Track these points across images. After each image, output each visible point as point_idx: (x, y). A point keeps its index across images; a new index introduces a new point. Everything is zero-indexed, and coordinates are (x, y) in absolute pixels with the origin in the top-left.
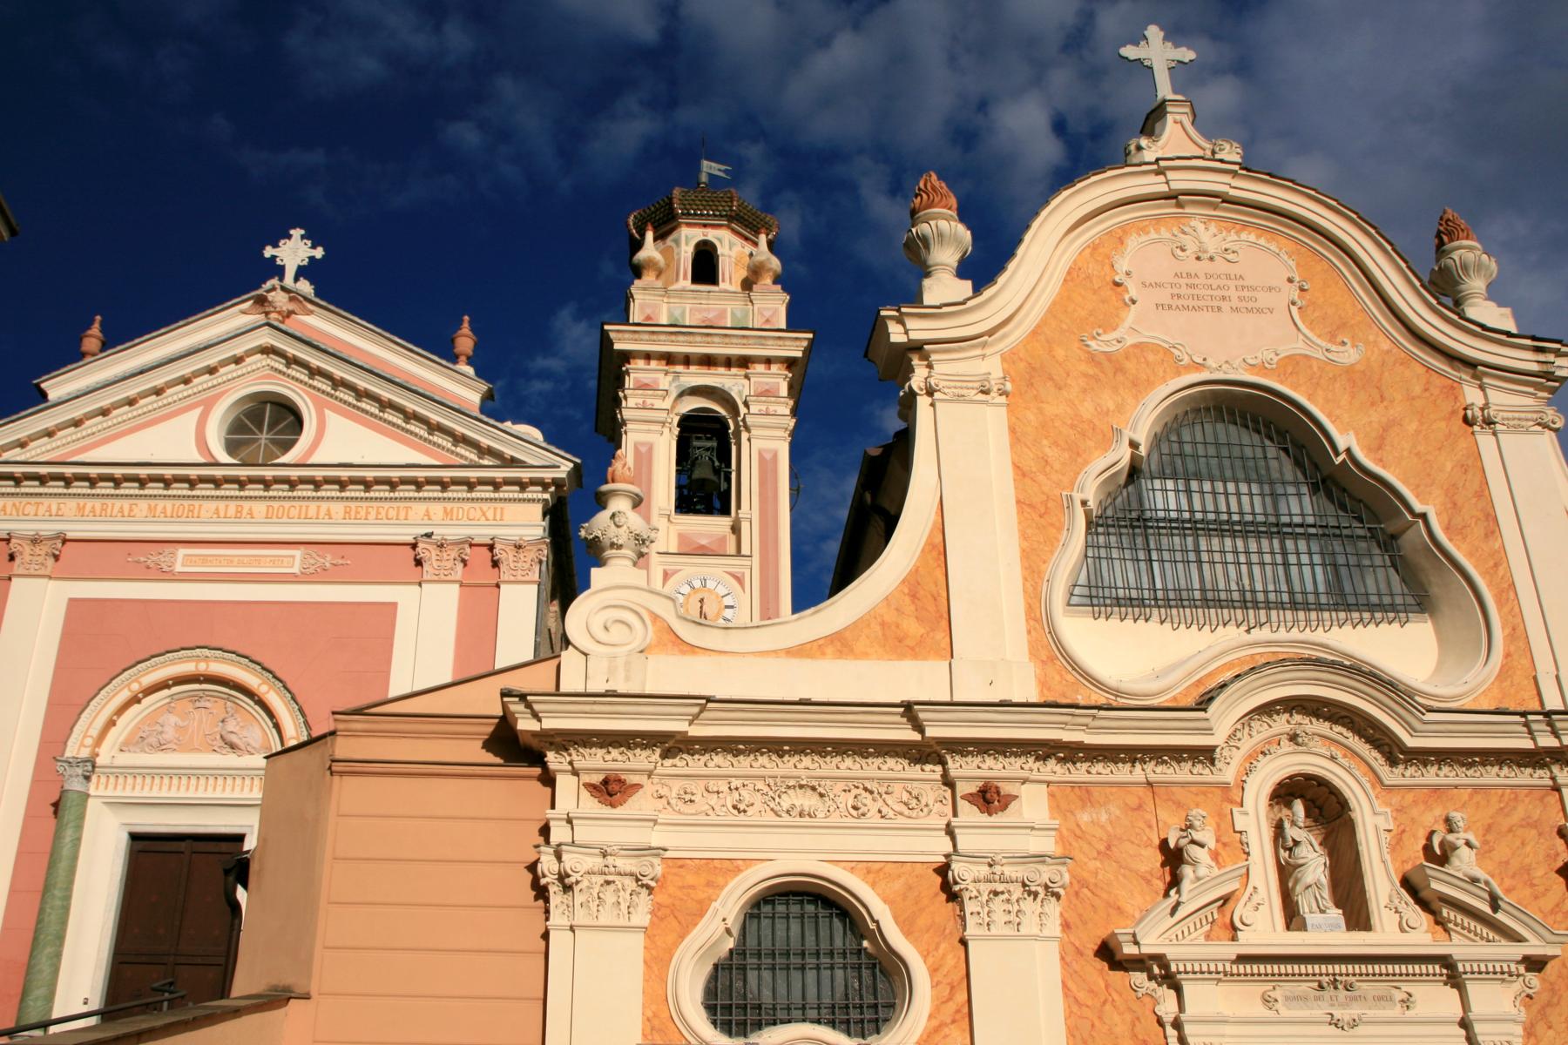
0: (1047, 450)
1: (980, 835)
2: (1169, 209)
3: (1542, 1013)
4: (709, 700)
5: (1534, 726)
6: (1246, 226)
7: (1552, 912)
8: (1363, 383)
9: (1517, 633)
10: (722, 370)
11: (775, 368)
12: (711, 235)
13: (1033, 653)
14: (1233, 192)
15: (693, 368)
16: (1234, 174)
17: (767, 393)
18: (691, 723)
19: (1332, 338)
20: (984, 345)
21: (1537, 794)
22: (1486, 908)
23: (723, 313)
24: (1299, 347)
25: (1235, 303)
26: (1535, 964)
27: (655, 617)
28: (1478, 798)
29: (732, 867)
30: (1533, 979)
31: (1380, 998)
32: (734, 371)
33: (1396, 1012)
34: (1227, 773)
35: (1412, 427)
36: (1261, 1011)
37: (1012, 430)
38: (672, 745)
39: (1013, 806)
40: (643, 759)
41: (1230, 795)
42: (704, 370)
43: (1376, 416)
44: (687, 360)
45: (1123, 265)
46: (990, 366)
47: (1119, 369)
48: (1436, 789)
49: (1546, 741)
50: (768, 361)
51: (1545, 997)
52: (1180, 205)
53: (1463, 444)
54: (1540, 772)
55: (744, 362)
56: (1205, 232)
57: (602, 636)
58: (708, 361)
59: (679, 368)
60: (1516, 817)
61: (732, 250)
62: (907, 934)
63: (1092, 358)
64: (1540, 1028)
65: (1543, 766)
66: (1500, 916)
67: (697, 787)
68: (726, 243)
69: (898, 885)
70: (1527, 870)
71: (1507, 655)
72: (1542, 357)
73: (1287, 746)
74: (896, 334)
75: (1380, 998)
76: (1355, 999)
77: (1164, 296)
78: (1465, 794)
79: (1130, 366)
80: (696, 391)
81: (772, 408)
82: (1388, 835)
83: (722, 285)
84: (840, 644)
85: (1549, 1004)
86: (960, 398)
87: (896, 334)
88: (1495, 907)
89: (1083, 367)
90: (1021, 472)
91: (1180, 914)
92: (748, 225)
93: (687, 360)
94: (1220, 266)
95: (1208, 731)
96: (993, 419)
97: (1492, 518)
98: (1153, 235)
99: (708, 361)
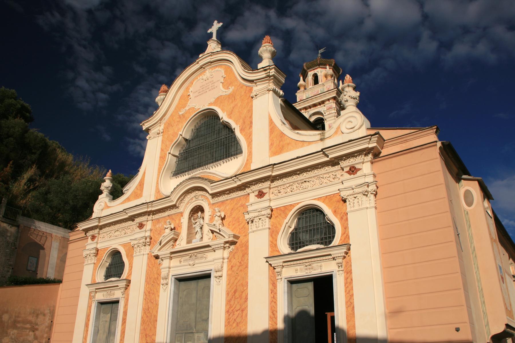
0: (167, 143)
1: (140, 234)
2: (202, 70)
3: (234, 255)
4: (100, 218)
5: (235, 180)
6: (216, 67)
7: (242, 228)
8: (231, 97)
9: (250, 153)
10: (319, 106)
11: (331, 101)
12: (315, 71)
13: (156, 191)
14: (212, 60)
15: (312, 109)
16: (211, 55)
17: (330, 108)
18: (99, 222)
19: (228, 88)
20: (160, 123)
21: (245, 197)
22: (218, 231)
23: (318, 91)
24: (221, 94)
25: (210, 88)
26: (233, 243)
27: (106, 202)
28: (232, 202)
29: (105, 249)
30: (232, 247)
31: (201, 257)
32: (322, 105)
33: (203, 260)
34: (181, 209)
35: (239, 105)
36: (178, 264)
37: (162, 141)
38: (101, 227)
39: (145, 227)
40: (97, 231)
41: (181, 214)
42: (315, 108)
43: (232, 105)
44: (310, 107)
45: (191, 89)
46: (160, 128)
47: (184, 117)
48: (223, 202)
49: (239, 183)
50: (329, 100)
51: (235, 251)
52: (204, 68)
53: (250, 104)
54: (245, 191)
55: (323, 102)
56: (208, 73)
57: (98, 209)
58: (315, 105)
59: (309, 110)
60: (239, 205)
61: (321, 72)
62: (127, 257)
63: (180, 117)
64: (232, 260)
65: (245, 189)
66: (221, 233)
67: (105, 234)
68: (320, 72)
69: (128, 247)
70: (238, 218)
71: (247, 160)
72: (266, 72)
73: (194, 199)
74: (144, 128)
75: (201, 257)
76: (196, 258)
77: (197, 94)
78: (229, 201)
79: (186, 115)
80: (314, 114)
81: (331, 112)
82: (210, 217)
83: (319, 83)
84: (128, 200)
85: (236, 253)
86: (154, 137)
87: (144, 128)
88: (220, 231)
89: (178, 120)
90: (162, 150)
91: (162, 245)
92: (322, 65)
93: (310, 107)
94: (210, 80)
95: (172, 201)
96: (160, 138)
97: (251, 123)
98: (199, 78)
99: (315, 105)
